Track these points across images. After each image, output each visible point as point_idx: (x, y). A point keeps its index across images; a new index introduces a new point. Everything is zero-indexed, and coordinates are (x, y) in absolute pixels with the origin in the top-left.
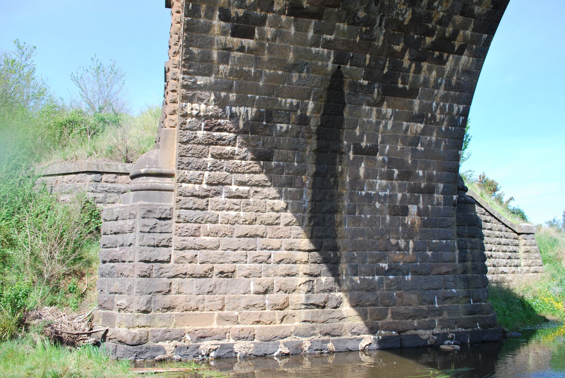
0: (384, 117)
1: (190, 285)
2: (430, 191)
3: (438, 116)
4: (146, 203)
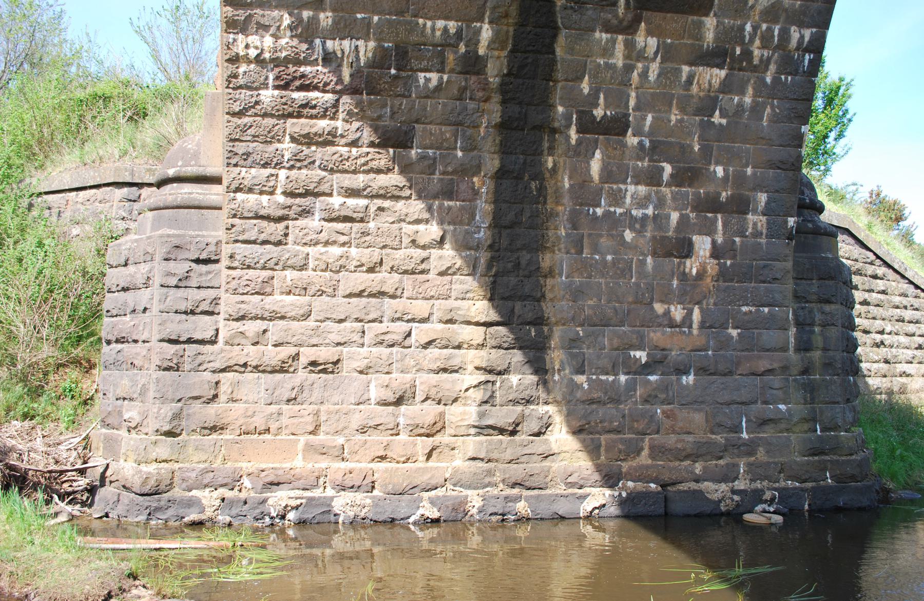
0: (641, 56)
2: (740, 206)
3: (756, 53)
4: (172, 232)
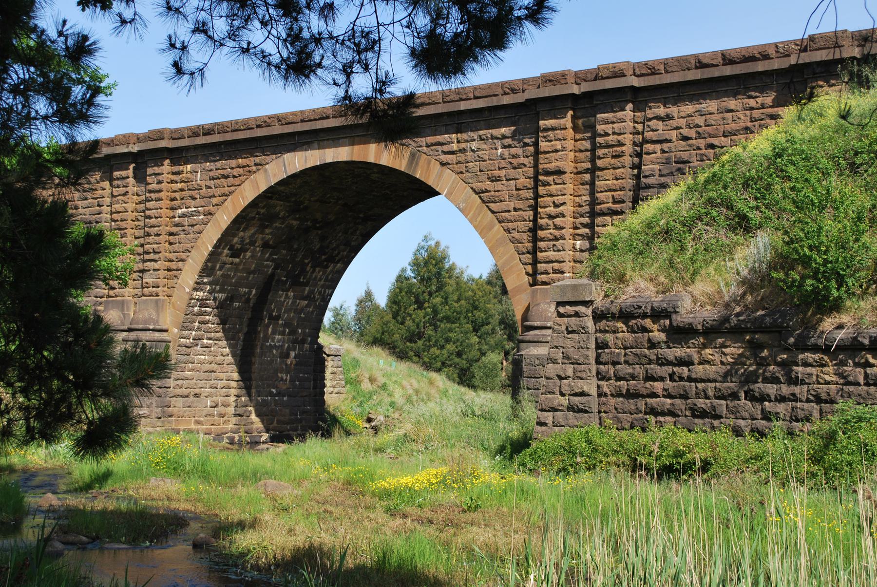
2: (303, 342)
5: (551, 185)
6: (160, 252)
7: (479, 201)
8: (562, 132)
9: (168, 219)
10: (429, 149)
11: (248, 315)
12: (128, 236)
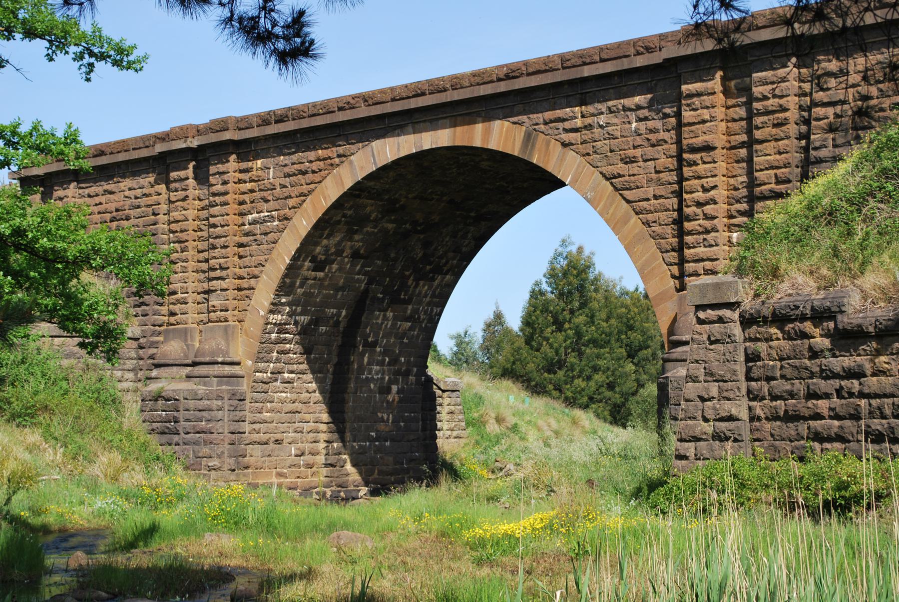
0: (387, 320)
1: (257, 450)
2: (407, 373)
3: (422, 317)
4: (230, 388)
5: (699, 164)
6: (228, 268)
7: (611, 188)
8: (710, 97)
9: (236, 227)
10: (547, 127)
11: (339, 340)
12: (190, 249)
